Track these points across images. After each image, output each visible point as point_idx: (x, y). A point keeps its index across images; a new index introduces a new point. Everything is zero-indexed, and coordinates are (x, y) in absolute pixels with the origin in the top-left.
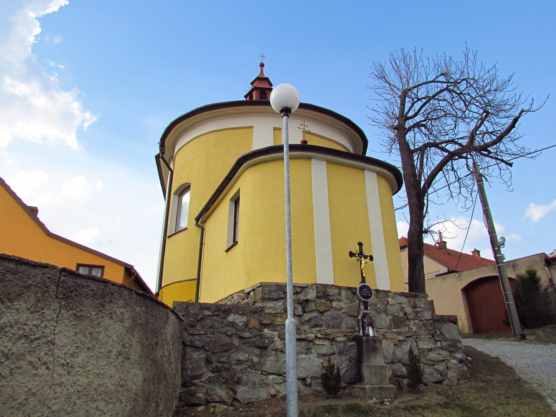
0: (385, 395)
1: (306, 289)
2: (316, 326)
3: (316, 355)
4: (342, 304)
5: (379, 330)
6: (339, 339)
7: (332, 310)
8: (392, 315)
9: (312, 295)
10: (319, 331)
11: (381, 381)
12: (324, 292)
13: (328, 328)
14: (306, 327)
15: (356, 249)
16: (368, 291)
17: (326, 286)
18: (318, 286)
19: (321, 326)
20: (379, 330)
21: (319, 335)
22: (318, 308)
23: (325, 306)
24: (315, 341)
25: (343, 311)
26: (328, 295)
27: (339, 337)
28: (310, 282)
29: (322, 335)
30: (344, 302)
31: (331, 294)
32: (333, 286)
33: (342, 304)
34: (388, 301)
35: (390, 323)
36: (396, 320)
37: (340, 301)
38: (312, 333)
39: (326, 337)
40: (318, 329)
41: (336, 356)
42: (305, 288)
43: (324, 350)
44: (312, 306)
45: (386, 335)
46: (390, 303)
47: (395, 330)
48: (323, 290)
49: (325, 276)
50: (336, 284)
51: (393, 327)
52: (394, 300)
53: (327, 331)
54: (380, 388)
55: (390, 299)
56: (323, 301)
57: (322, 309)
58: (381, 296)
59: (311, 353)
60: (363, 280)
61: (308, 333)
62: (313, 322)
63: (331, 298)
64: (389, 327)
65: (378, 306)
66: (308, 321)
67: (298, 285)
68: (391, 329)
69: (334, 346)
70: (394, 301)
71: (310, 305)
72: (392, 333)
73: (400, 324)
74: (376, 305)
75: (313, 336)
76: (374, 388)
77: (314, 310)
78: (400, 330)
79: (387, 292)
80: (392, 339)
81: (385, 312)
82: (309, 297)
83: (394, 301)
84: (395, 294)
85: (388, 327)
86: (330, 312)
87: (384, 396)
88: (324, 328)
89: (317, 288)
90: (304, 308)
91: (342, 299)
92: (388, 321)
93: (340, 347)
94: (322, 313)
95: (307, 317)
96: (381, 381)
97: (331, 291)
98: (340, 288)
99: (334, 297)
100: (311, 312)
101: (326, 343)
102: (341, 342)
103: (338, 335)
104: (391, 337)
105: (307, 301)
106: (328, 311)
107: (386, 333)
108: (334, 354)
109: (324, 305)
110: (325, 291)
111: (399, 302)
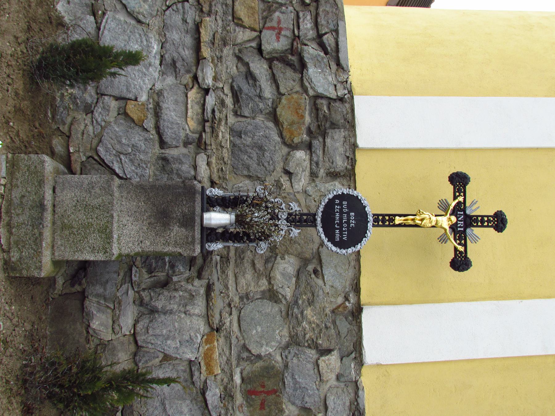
0: (18, 227)
1: (334, 66)
2: (236, 95)
3: (158, 86)
4: (302, 181)
5: (235, 313)
6: (202, 160)
7: (285, 150)
8: (286, 366)
9: (320, 79)
10: (223, 103)
11: (64, 227)
12: (333, 117)
13: (232, 131)
14: (231, 66)
15: (481, 203)
16: (351, 231)
17: (350, 124)
18: (346, 100)
19: (236, 114)
20: (235, 313)
21: (211, 100)
22: (284, 101)
23: (292, 124)
24: (195, 90)
25: (284, 179)
26: (324, 135)
27: (208, 164)
28: (356, 76)
29: (213, 111)
30: (309, 189)
31: (328, 141)
32: (354, 146)
33: (302, 181)
34: (328, 351)
35: (259, 357)
36: (270, 385)
37: (313, 175)
38: (215, 79)
39: (208, 121)
40: (229, 101)
41: (157, 149)
42: (338, 64)
43: (171, 112)
44: (288, 80)
45: (222, 340)
46: (323, 361)
47: (237, 379)
48: (338, 118)
49: (377, 122)
50: (359, 156)
51: (248, 368)
52: (333, 382)
53: (222, 128)
54: (42, 206)
55: (333, 359)
56: (308, 119)
57: (285, 114)
58: (344, 326)
59: (163, 73)
60: (385, 220)
61: (216, 66)
62: (245, 87)
63: (316, 143)
64: (246, 354)
65: (308, 312)
66: (250, 76)
67: (341, 39)
68: (239, 359)
69: (184, 150)
70: (331, 377)
71: (289, 73)
72: (228, 361)
73: (258, 400)
74: (311, 303)
75: (209, 81)
76: (41, 183)
77: (278, 87)
78: (239, 399)
79: (356, 351)
80: (208, 356)
81: (294, 341)
82: (312, 71)
83: (331, 377)
84: (356, 387)
85: (245, 348)
86: (277, 139)
87: (16, 220)
88: (232, 120)
89: (341, 99)
90: (283, 59)
91: (317, 181)
92: (264, 350)
93: (181, 163)
94: (274, 117)
95: (259, 68)
96: (64, 227)
97: (336, 141)
98: (350, 175)
99: (320, 153)
100: (274, 79)
101: (193, 124)
102: (195, 167)
103: (213, 160)
104: (216, 355)
105: (302, 66)
106: (281, 135)
107: (228, 338)
108: (163, 144)
109: (295, 118)
110: (334, 126)
111: (330, 403)
